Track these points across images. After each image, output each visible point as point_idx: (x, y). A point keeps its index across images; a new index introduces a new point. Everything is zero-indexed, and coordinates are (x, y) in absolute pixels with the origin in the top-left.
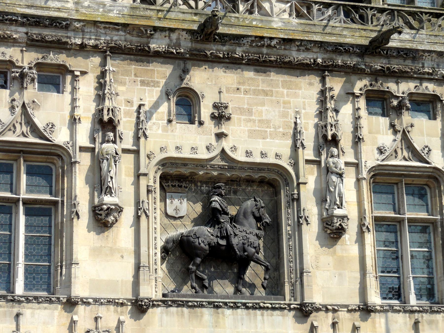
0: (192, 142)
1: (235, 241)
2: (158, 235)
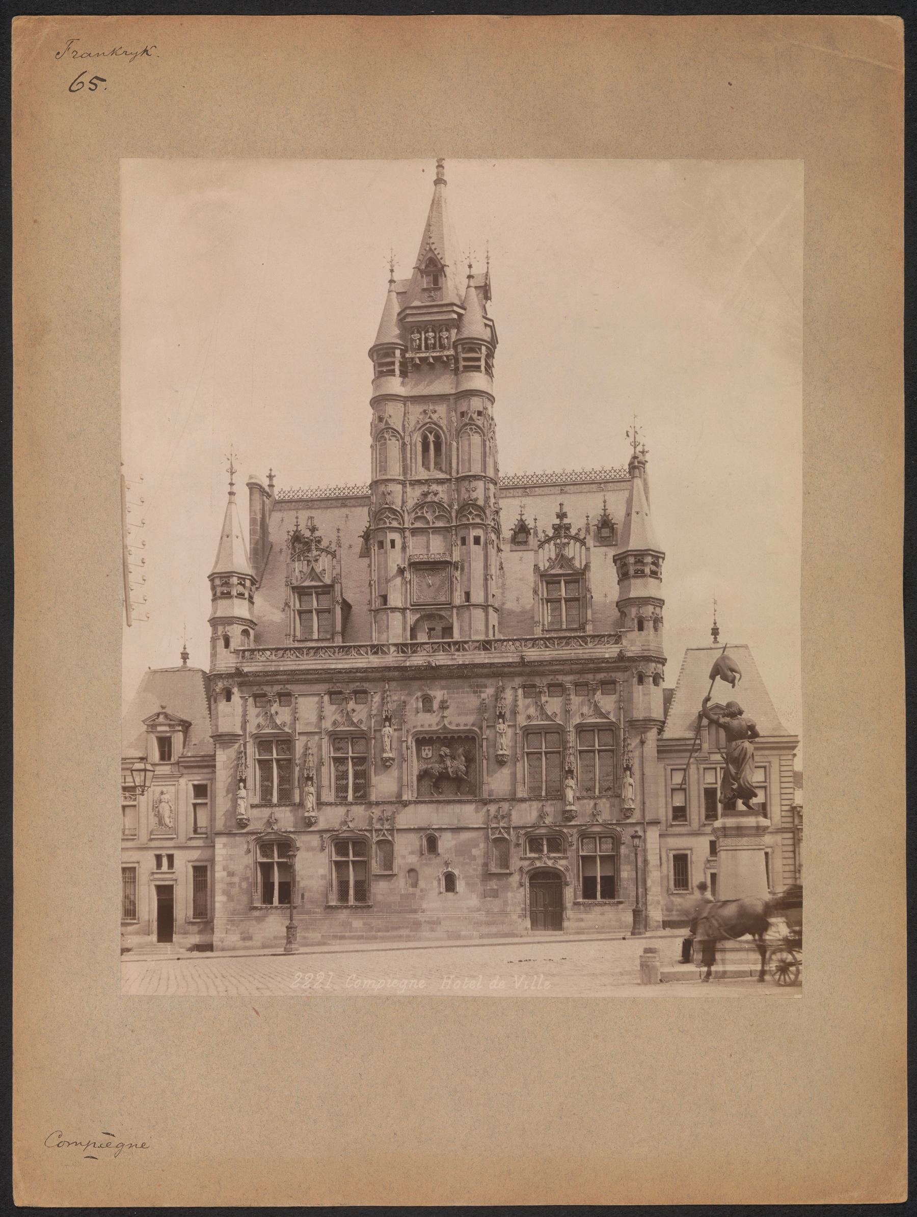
0: (428, 722)
1: (450, 770)
2: (415, 767)
